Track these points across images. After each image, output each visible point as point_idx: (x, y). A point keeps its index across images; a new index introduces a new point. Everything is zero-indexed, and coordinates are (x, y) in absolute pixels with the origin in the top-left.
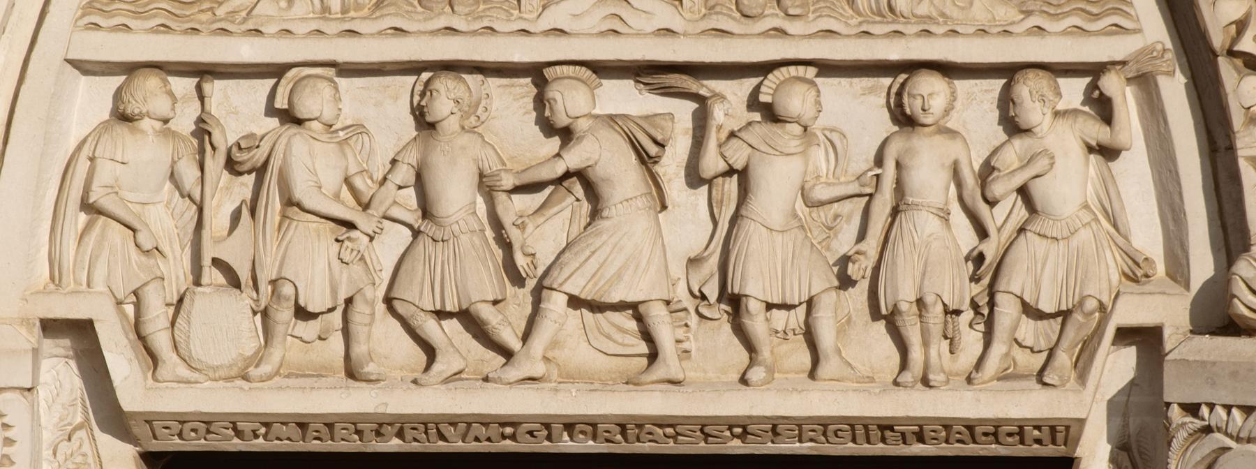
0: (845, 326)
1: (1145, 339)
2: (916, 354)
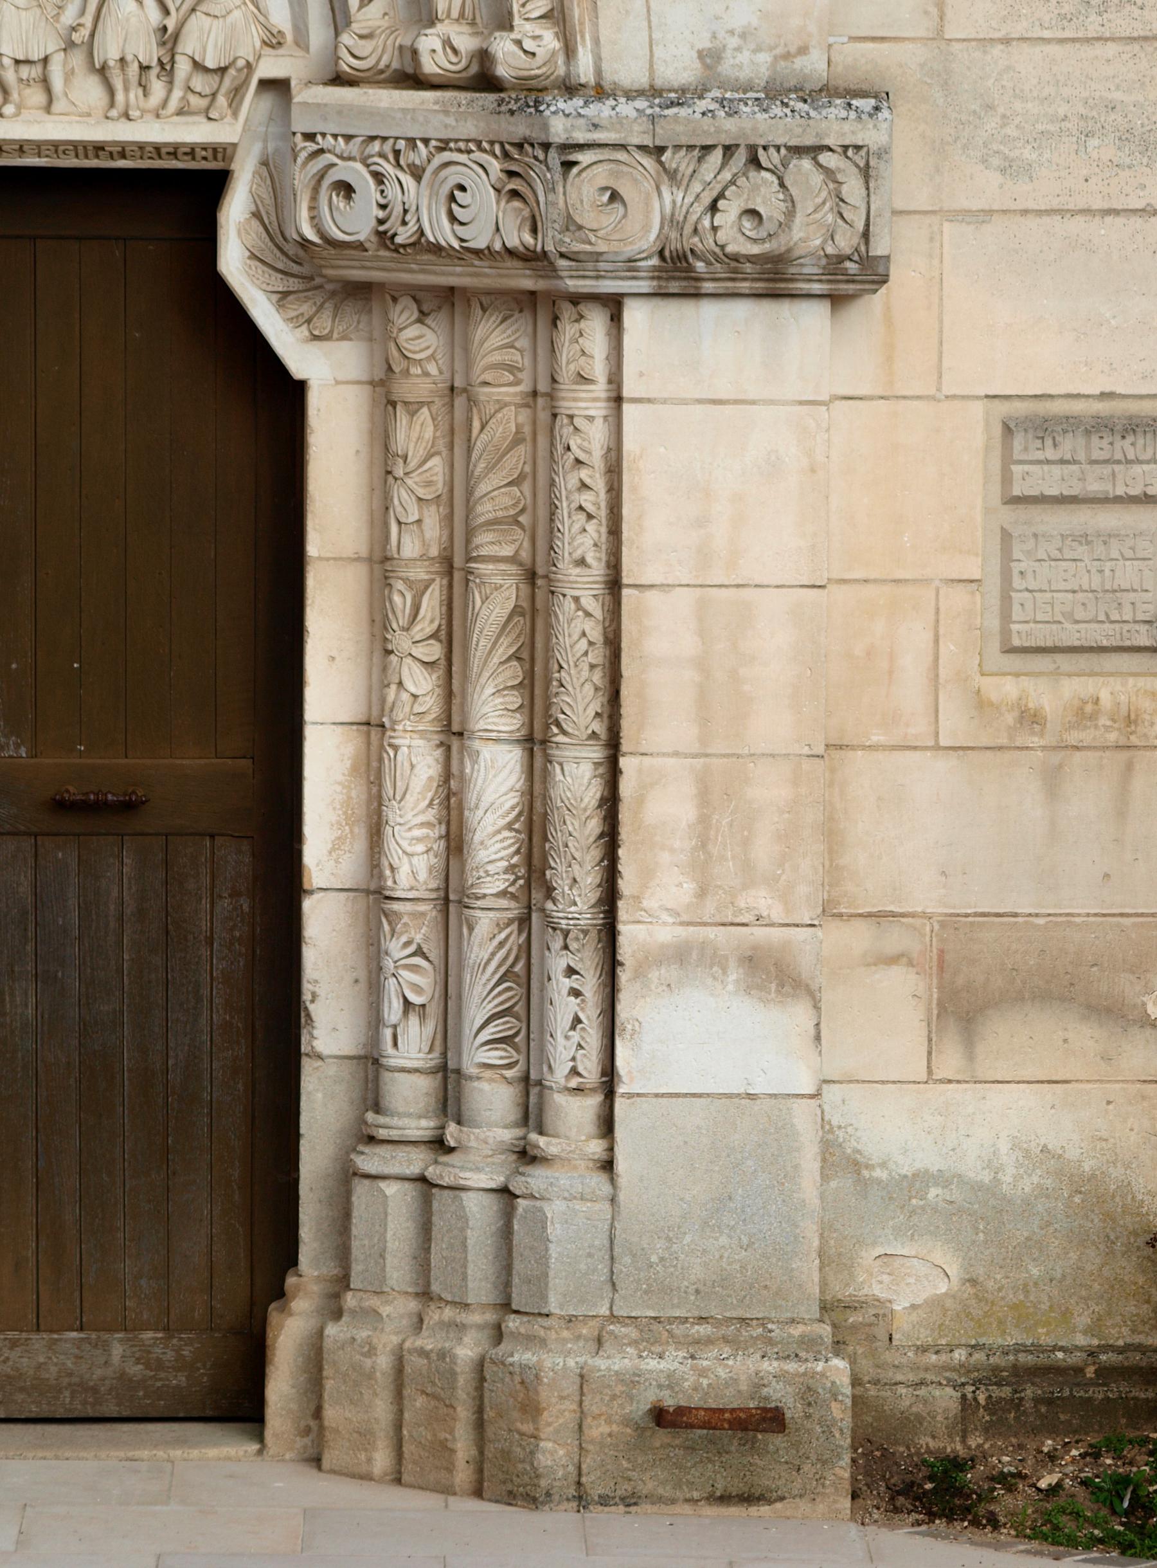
0: (69, 75)
1: (278, 87)
2: (120, 97)
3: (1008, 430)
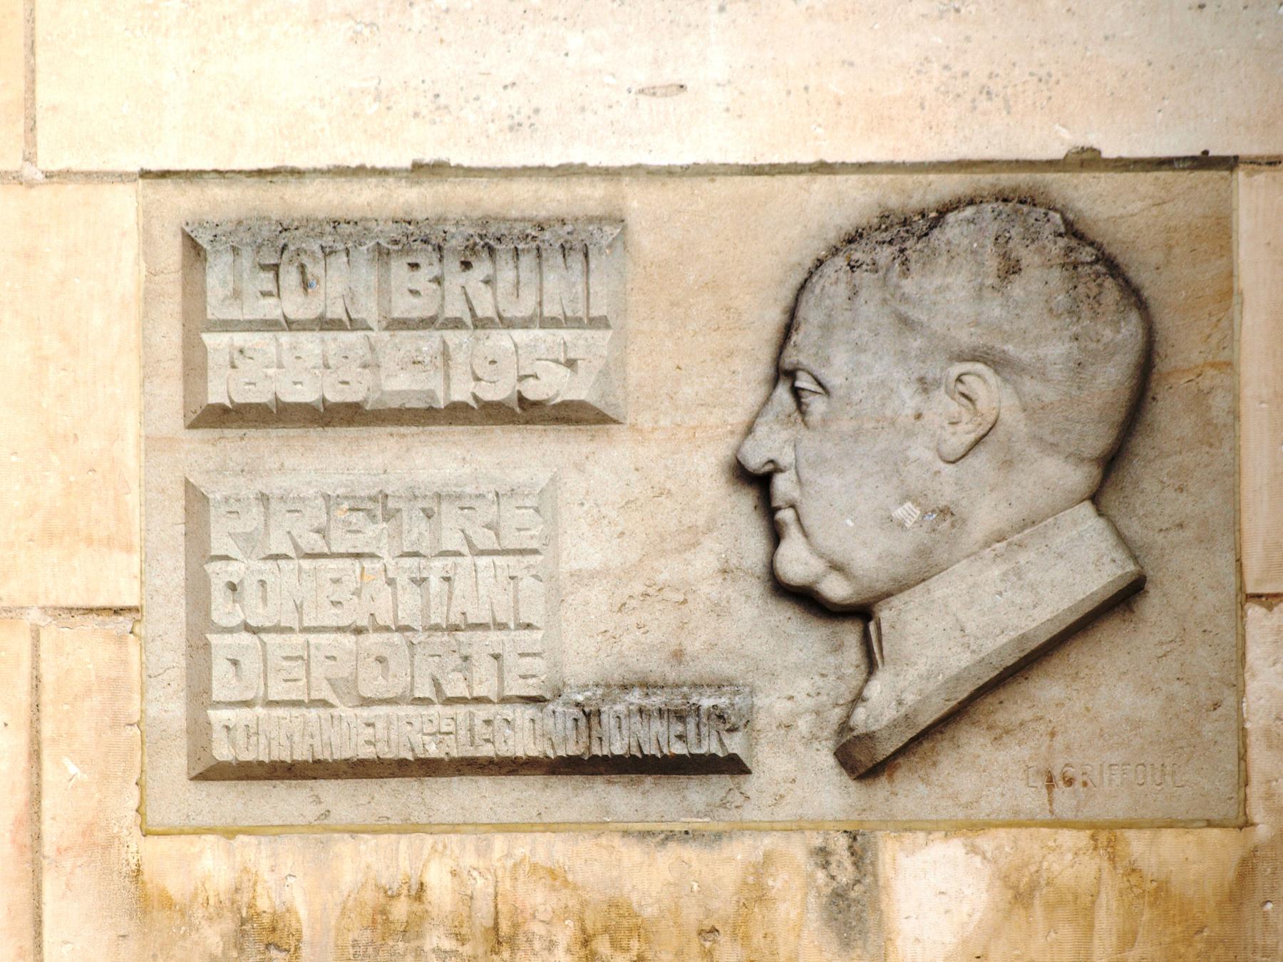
3: (194, 250)
